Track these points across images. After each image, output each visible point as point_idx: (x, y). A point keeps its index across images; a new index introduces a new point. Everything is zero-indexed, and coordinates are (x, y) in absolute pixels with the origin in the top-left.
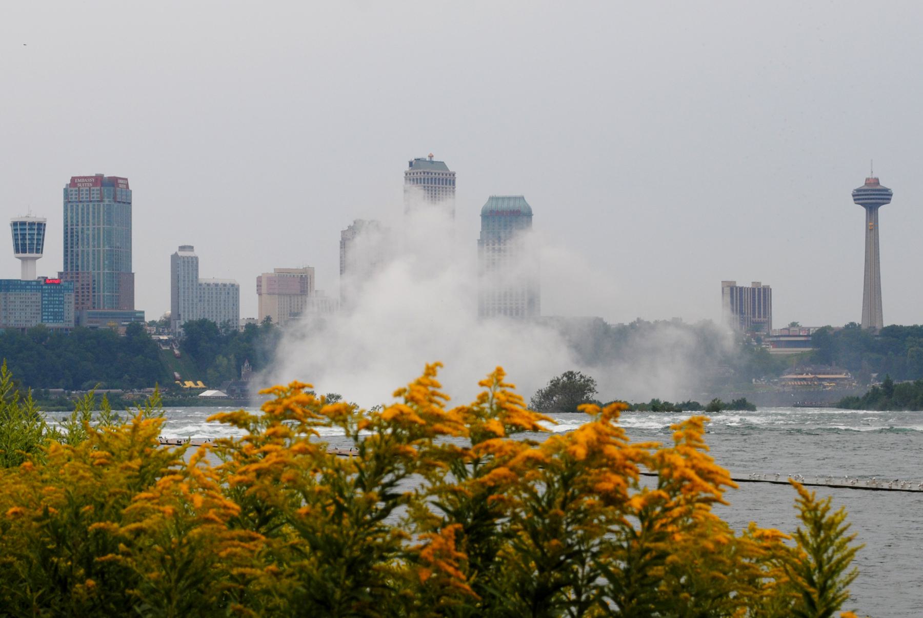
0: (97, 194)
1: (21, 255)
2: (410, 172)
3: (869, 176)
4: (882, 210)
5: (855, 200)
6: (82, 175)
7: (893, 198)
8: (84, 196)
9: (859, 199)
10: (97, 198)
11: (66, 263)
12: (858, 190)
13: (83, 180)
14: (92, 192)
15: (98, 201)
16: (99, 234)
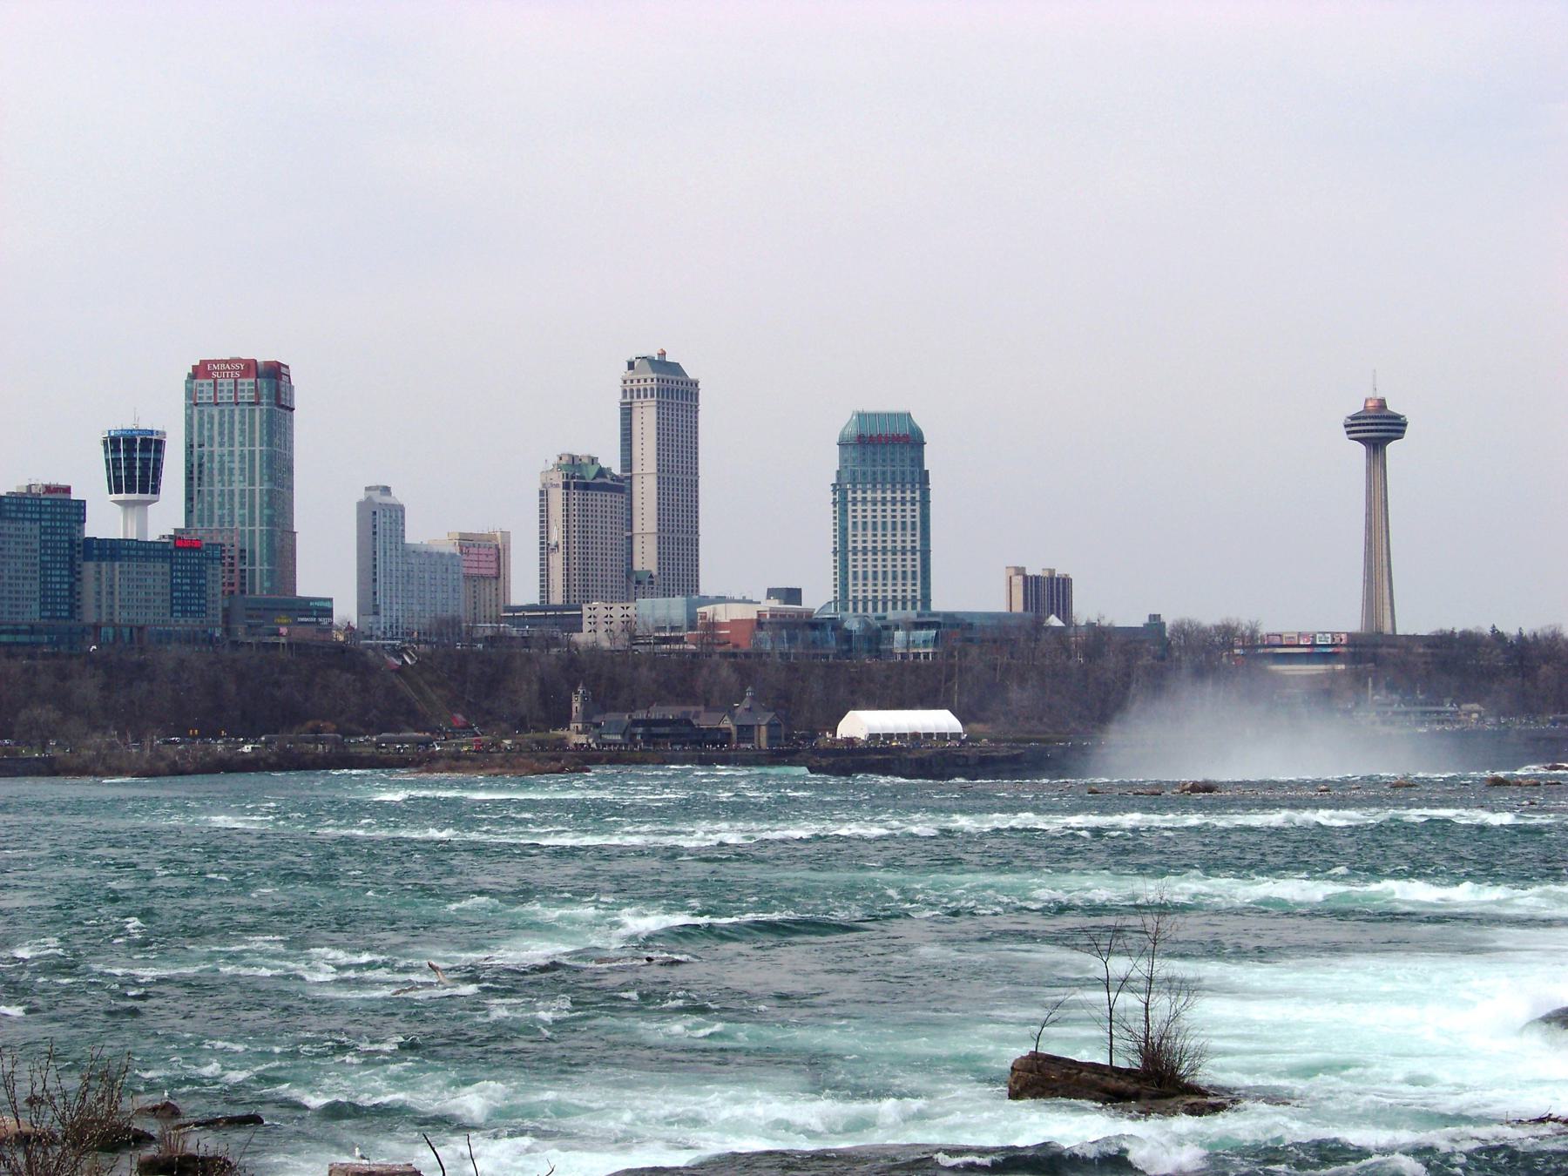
0: (249, 391)
1: (123, 496)
2: (632, 378)
3: (1370, 395)
4: (1391, 448)
5: (1348, 433)
6: (218, 358)
7: (1408, 429)
8: (225, 394)
9: (1354, 432)
10: (249, 397)
11: (189, 512)
12: (1353, 418)
14: (239, 387)
15: (250, 404)
16: (252, 460)
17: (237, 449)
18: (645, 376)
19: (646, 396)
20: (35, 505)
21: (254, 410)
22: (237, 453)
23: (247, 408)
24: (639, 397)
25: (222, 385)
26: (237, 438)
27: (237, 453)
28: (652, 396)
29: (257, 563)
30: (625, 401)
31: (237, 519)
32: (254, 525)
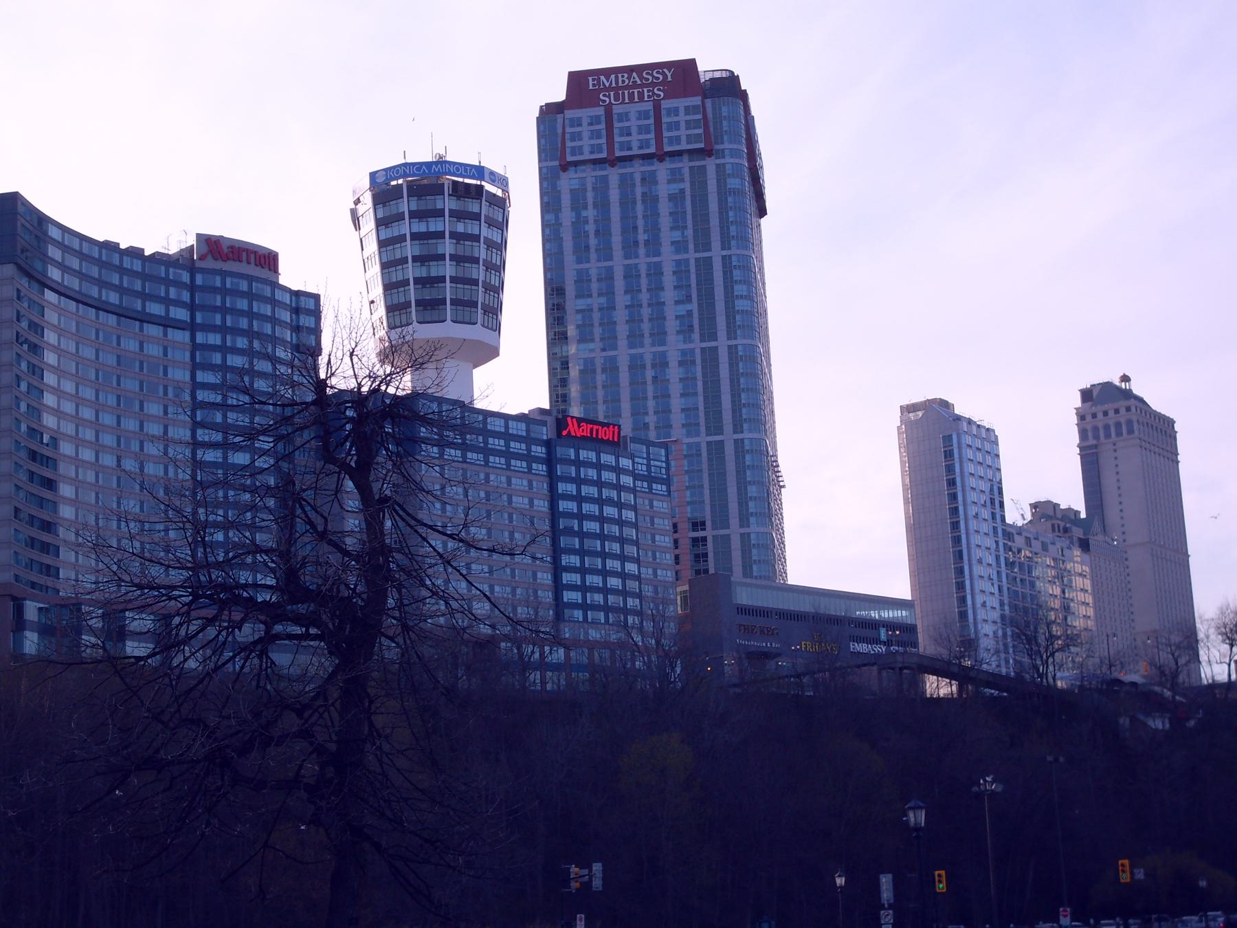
8: (635, 138)
10: (689, 139)
13: (623, 79)
14: (665, 120)
15: (690, 152)
17: (668, 257)
18: (1116, 405)
19: (1119, 434)
20: (178, 284)
21: (704, 167)
22: (668, 269)
23: (685, 164)
24: (1108, 436)
25: (624, 117)
26: (667, 236)
27: (668, 269)
28: (1131, 431)
29: (734, 521)
30: (1086, 444)
31: (677, 418)
32: (719, 430)
